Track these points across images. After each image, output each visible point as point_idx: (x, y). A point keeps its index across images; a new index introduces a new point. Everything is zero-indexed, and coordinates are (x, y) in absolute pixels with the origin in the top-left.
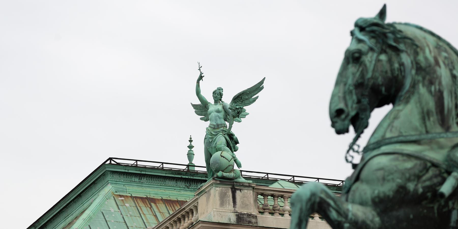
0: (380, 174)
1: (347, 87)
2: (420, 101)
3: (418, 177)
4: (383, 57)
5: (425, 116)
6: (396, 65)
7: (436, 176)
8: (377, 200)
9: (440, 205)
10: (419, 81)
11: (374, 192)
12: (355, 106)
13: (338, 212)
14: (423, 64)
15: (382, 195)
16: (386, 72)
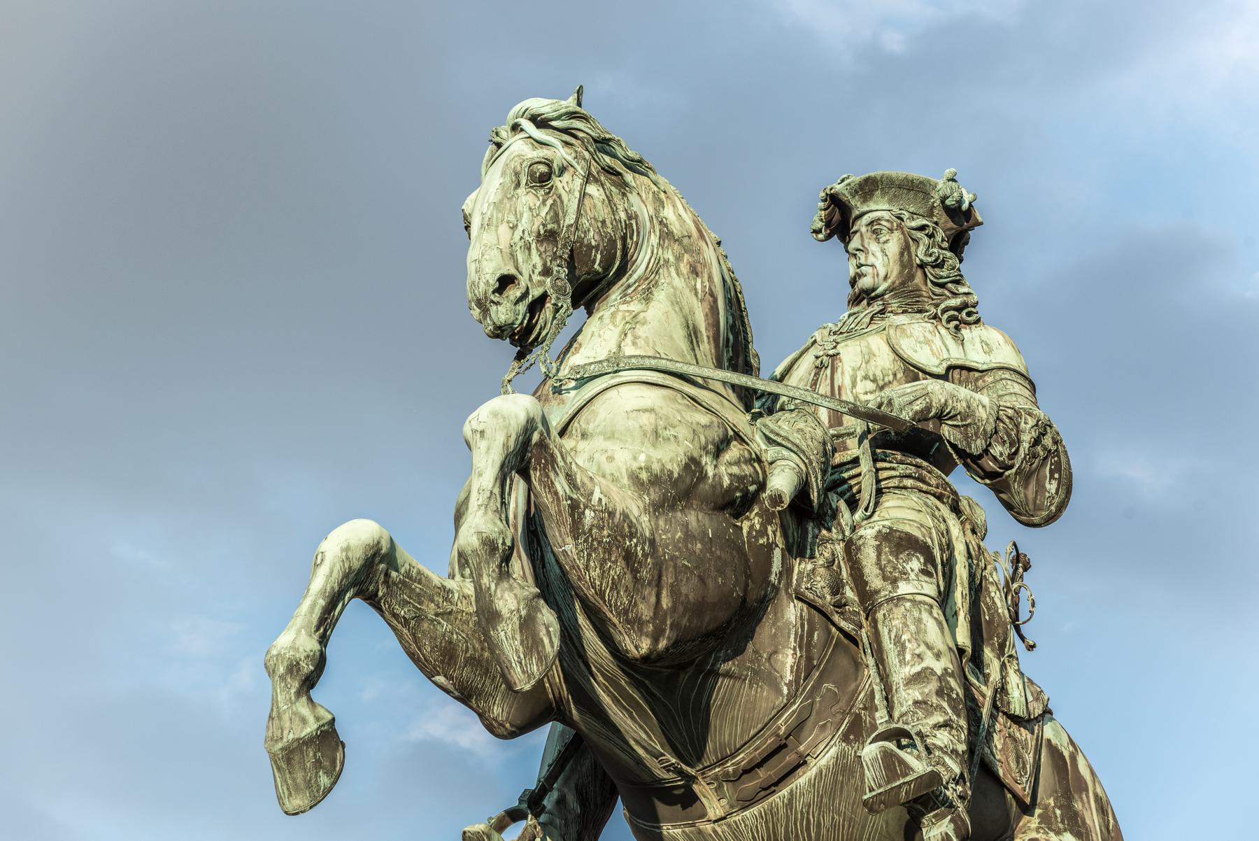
0: (647, 420)
1: (518, 233)
2: (676, 302)
3: (718, 451)
4: (592, 189)
5: (693, 335)
6: (623, 216)
7: (749, 461)
8: (644, 476)
9: (752, 527)
10: (667, 261)
11: (635, 458)
12: (536, 278)
13: (570, 478)
14: (676, 228)
15: (656, 467)
16: (603, 222)
